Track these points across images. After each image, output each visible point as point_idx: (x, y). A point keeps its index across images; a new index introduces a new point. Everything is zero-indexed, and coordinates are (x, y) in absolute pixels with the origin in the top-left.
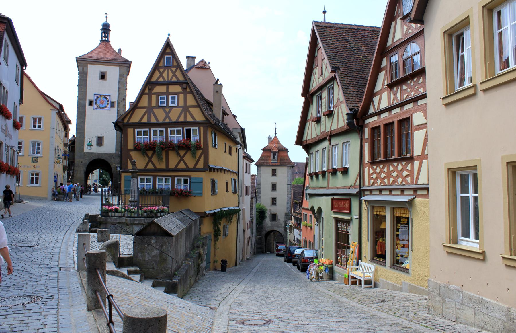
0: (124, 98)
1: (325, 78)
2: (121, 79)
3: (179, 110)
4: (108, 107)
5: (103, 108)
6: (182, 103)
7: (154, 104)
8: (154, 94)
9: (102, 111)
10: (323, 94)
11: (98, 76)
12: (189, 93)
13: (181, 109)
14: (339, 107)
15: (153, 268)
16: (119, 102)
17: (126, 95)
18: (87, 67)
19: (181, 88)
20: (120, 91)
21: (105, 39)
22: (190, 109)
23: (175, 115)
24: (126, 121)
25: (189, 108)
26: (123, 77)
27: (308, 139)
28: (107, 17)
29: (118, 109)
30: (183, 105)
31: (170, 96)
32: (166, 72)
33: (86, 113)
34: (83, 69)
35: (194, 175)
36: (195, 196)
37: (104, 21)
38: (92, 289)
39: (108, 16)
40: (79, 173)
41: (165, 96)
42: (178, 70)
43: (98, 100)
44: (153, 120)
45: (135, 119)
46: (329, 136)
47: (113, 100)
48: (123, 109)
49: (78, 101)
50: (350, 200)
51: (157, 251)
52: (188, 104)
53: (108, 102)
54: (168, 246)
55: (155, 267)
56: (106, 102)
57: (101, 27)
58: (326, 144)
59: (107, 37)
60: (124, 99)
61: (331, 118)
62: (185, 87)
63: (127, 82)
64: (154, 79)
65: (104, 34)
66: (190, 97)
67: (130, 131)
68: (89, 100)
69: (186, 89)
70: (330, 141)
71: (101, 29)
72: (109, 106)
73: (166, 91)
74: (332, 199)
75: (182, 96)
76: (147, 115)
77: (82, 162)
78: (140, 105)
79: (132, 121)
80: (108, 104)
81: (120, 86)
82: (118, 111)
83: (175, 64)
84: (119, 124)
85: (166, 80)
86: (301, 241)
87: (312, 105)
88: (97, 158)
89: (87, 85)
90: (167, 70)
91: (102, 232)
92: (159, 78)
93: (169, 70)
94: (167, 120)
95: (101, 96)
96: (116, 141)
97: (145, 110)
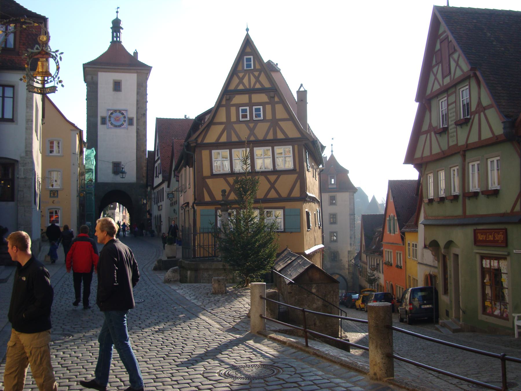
1: (456, 77)
3: (266, 125)
4: (125, 125)
5: (120, 126)
6: (269, 116)
7: (233, 119)
8: (234, 105)
9: (118, 130)
10: (449, 98)
11: (111, 86)
12: (277, 103)
13: (268, 124)
14: (482, 114)
15: (315, 324)
18: (97, 75)
19: (267, 97)
21: (117, 39)
22: (280, 123)
23: (261, 131)
24: (199, 141)
25: (279, 122)
27: (424, 155)
28: (117, 12)
29: (138, 127)
30: (271, 118)
31: (254, 108)
32: (246, 78)
34: (92, 78)
35: (288, 205)
36: (291, 232)
37: (115, 18)
38: (382, 352)
39: (119, 10)
41: (248, 108)
42: (263, 74)
43: (112, 116)
44: (234, 139)
45: (211, 137)
46: (463, 151)
50: (506, 230)
51: (319, 303)
52: (278, 117)
53: (125, 119)
54: (333, 295)
55: (318, 323)
56: (123, 119)
57: (111, 26)
58: (458, 159)
59: (119, 37)
60: (144, 115)
61: (466, 129)
62: (273, 96)
63: (148, 93)
64: (232, 87)
65: (115, 34)
66: (279, 108)
67: (205, 153)
69: (274, 97)
70: (464, 157)
71: (111, 28)
72: (125, 124)
73: (248, 102)
74: (475, 230)
75: (269, 107)
76: (225, 132)
78: (217, 120)
79: (207, 141)
80: (125, 121)
83: (258, 67)
84: (192, 145)
85: (248, 88)
86: (381, 286)
87: (430, 111)
90: (247, 75)
91: (219, 282)
92: (238, 85)
93: (251, 75)
94: (252, 138)
95: (115, 111)
97: (222, 127)
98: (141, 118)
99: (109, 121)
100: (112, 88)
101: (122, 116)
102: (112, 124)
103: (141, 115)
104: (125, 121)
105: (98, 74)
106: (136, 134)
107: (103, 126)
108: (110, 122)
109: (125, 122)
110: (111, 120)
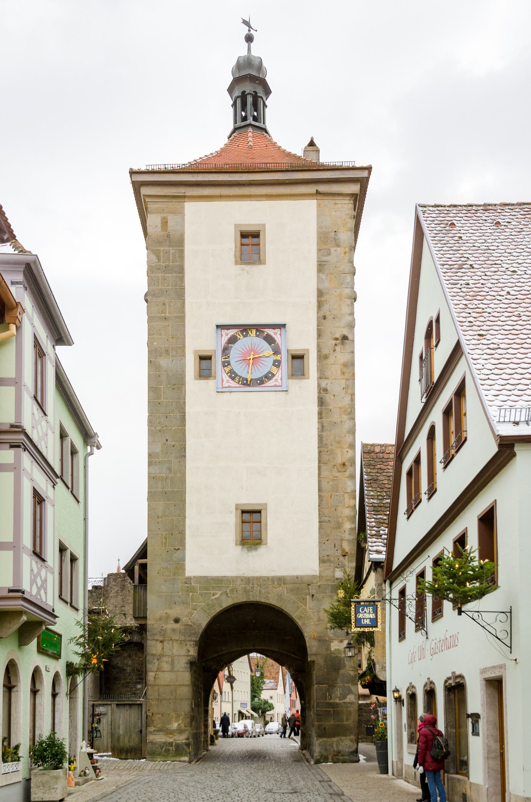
0: (346, 332)
2: (329, 254)
4: (278, 376)
5: (261, 381)
16: (325, 351)
17: (354, 320)
18: (181, 213)
20: (326, 307)
26: (338, 246)
29: (323, 385)
33: (189, 410)
34: (165, 223)
40: (166, 666)
47: (297, 347)
48: (343, 383)
49: (150, 362)
53: (278, 357)
68: (196, 352)
77: (177, 621)
81: (326, 285)
82: (322, 391)
88: (241, 598)
89: (183, 289)
96: (320, 522)
98: (335, 350)
99: (224, 366)
100: (233, 253)
101: (267, 349)
102: (233, 375)
103: (334, 342)
104: (277, 364)
105: (183, 208)
106: (315, 409)
107: (203, 382)
108: (227, 369)
109: (278, 366)
110: (229, 364)
